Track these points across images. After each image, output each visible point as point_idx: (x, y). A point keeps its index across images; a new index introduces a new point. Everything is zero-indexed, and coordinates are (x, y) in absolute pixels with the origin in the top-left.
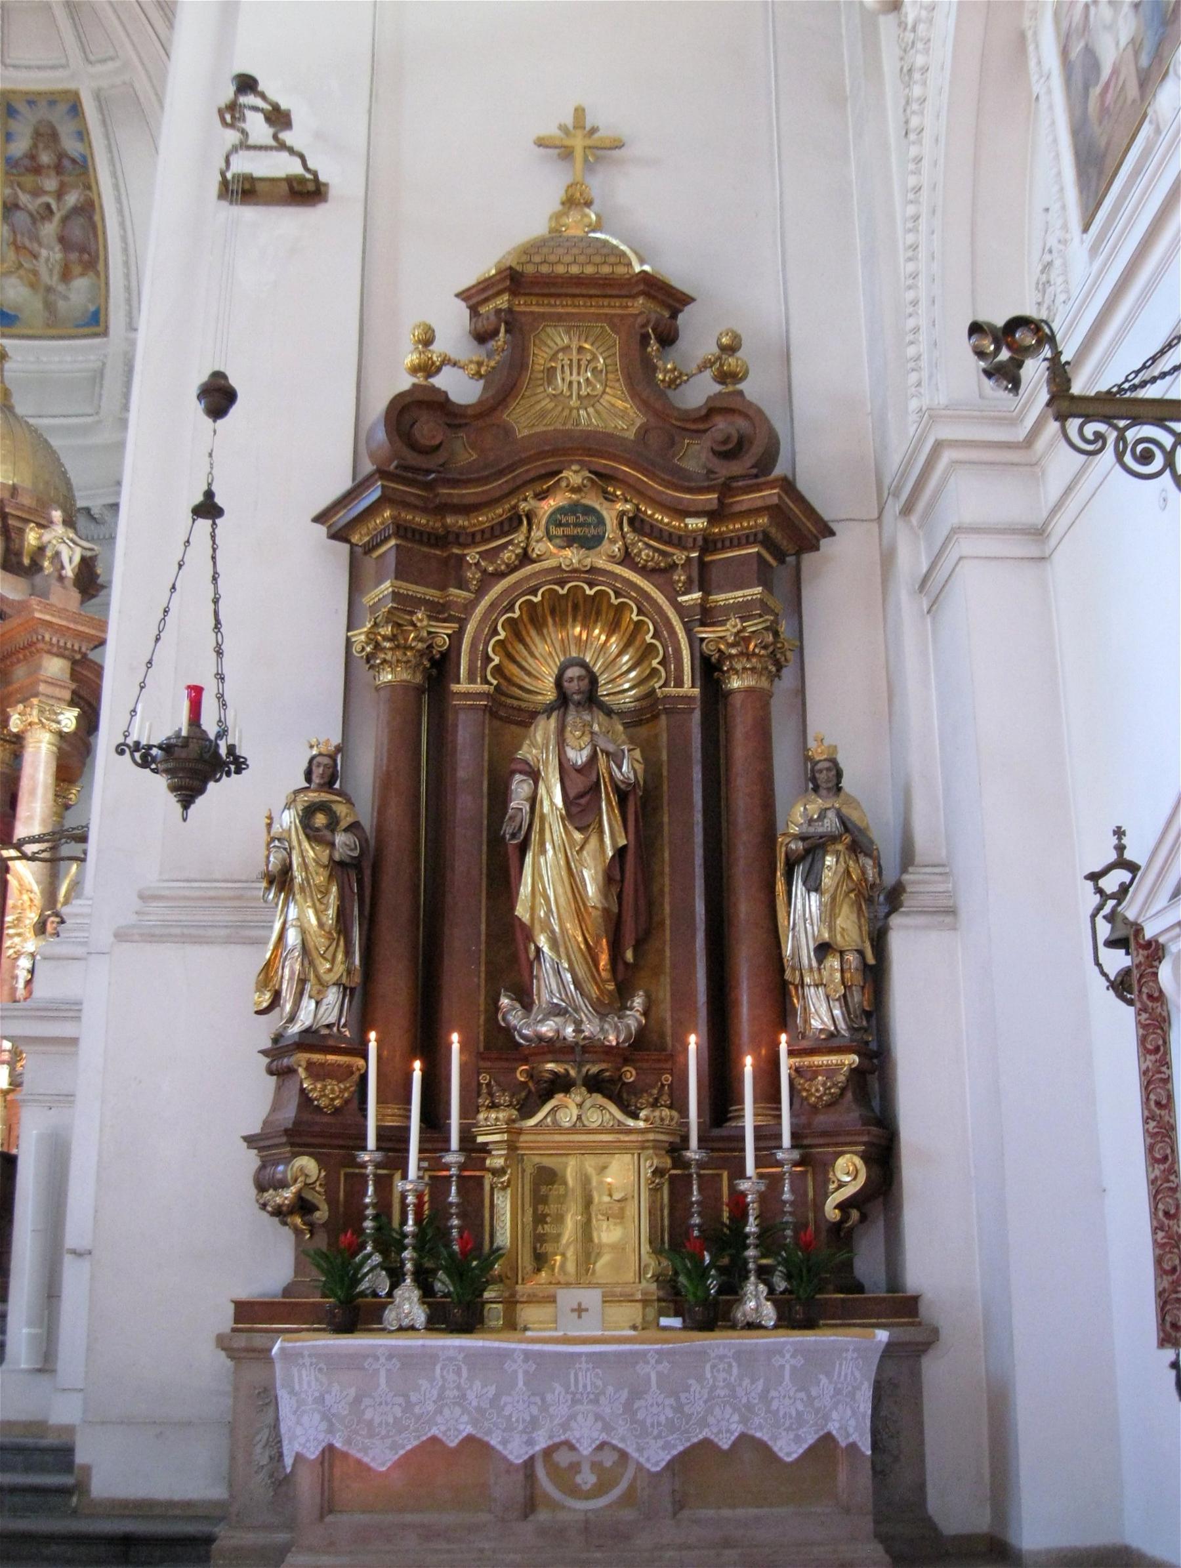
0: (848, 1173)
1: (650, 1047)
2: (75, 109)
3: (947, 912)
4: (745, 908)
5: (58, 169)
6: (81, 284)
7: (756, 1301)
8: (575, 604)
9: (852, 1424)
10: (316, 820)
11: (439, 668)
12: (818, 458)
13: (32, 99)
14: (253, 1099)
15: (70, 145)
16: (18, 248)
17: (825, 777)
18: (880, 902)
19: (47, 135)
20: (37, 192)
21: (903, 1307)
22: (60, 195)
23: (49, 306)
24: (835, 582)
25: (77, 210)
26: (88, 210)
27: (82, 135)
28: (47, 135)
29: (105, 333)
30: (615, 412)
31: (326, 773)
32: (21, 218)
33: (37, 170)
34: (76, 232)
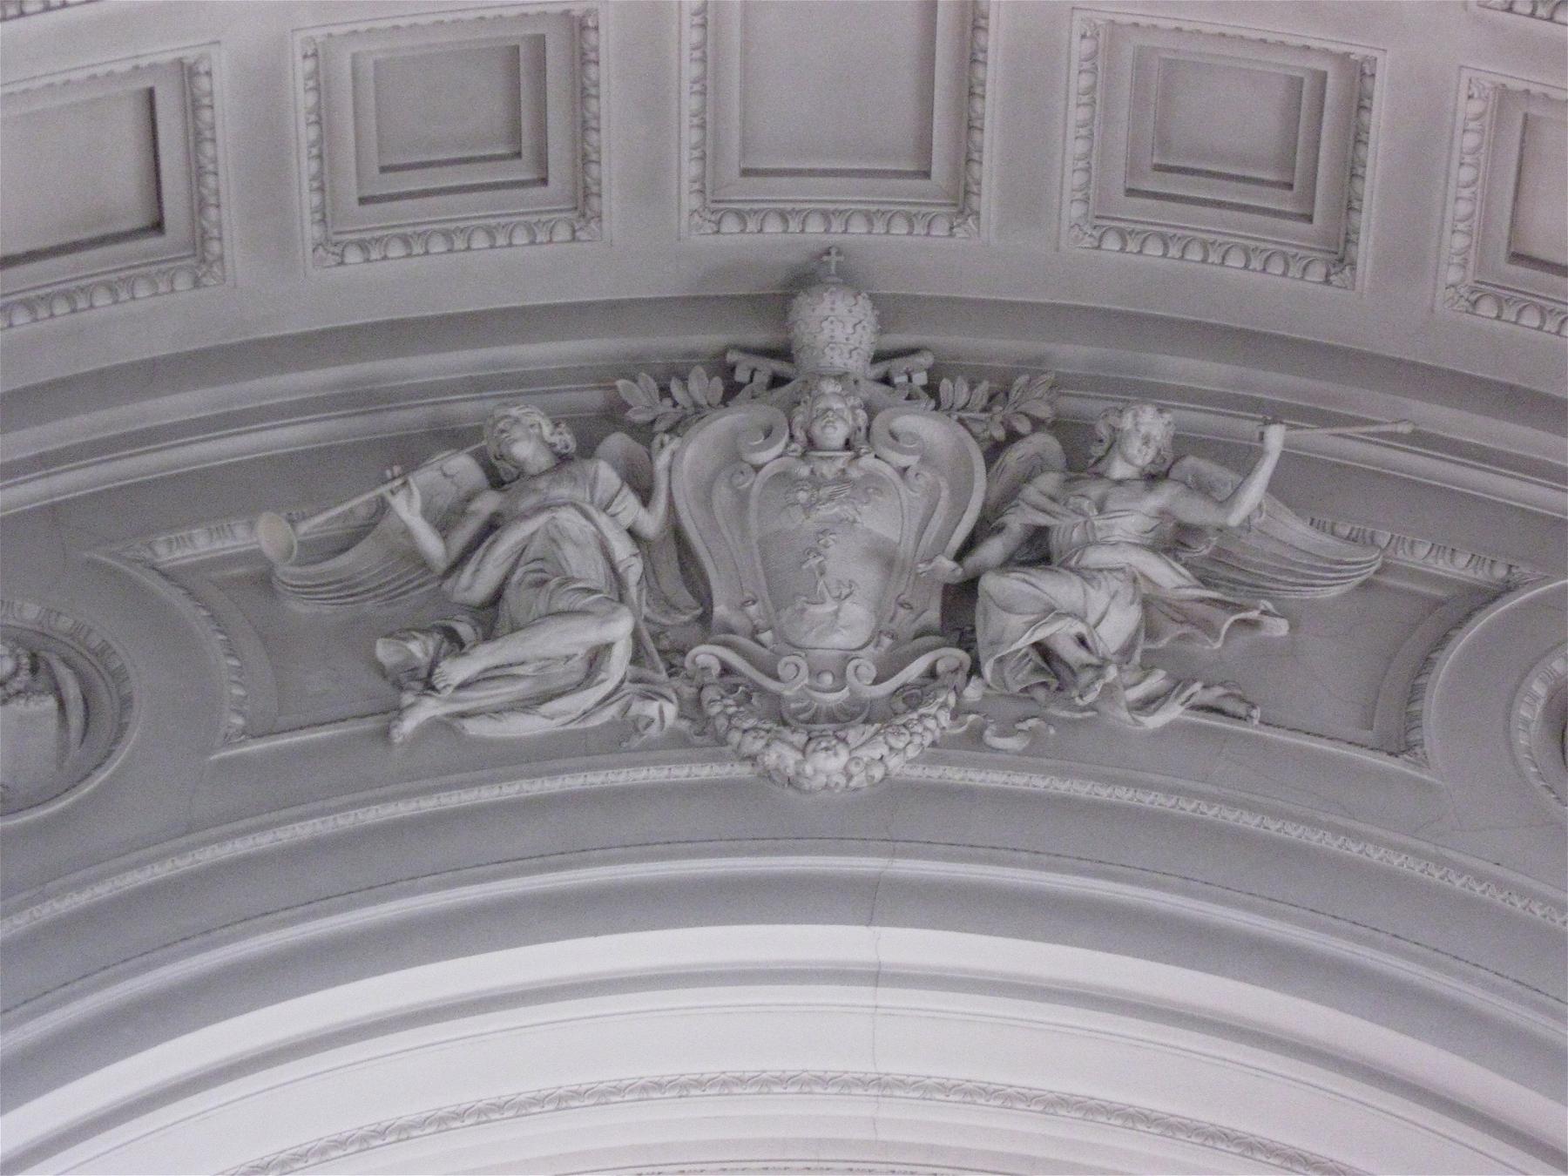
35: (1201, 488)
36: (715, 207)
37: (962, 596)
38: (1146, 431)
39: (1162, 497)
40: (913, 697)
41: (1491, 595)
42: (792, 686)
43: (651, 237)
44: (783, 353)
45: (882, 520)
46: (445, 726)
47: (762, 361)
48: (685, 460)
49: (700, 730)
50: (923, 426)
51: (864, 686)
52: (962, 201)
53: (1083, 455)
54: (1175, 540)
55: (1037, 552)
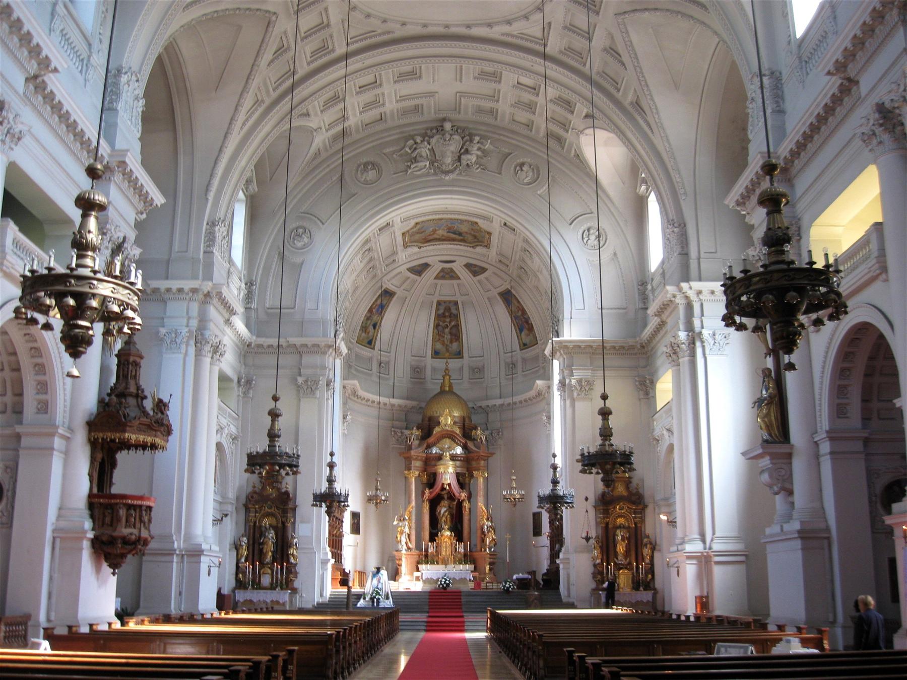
1: (630, 564)
2: (456, 303)
3: (660, 550)
4: (639, 550)
5: (450, 317)
6: (455, 345)
7: (641, 589)
8: (621, 516)
9: (650, 599)
11: (607, 524)
13: (445, 302)
14: (591, 569)
15: (454, 311)
16: (439, 335)
17: (648, 537)
18: (653, 549)
19: (448, 309)
20: (444, 322)
21: (655, 589)
22: (450, 323)
23: (447, 350)
25: (454, 326)
26: (458, 326)
27: (458, 309)
28: (448, 309)
29: (462, 357)
30: (625, 494)
31: (597, 537)
32: (440, 328)
33: (445, 317)
34: (454, 331)
35: (482, 144)
36: (435, 113)
38: (477, 139)
39: (479, 145)
40: (455, 169)
41: (510, 154)
42: (444, 168)
43: (429, 115)
44: (442, 126)
45: (452, 148)
46: (412, 173)
48: (433, 141)
49: (435, 174)
50: (457, 137)
51: (451, 168)
52: (459, 113)
53: (471, 141)
54: (479, 149)
55: (467, 152)
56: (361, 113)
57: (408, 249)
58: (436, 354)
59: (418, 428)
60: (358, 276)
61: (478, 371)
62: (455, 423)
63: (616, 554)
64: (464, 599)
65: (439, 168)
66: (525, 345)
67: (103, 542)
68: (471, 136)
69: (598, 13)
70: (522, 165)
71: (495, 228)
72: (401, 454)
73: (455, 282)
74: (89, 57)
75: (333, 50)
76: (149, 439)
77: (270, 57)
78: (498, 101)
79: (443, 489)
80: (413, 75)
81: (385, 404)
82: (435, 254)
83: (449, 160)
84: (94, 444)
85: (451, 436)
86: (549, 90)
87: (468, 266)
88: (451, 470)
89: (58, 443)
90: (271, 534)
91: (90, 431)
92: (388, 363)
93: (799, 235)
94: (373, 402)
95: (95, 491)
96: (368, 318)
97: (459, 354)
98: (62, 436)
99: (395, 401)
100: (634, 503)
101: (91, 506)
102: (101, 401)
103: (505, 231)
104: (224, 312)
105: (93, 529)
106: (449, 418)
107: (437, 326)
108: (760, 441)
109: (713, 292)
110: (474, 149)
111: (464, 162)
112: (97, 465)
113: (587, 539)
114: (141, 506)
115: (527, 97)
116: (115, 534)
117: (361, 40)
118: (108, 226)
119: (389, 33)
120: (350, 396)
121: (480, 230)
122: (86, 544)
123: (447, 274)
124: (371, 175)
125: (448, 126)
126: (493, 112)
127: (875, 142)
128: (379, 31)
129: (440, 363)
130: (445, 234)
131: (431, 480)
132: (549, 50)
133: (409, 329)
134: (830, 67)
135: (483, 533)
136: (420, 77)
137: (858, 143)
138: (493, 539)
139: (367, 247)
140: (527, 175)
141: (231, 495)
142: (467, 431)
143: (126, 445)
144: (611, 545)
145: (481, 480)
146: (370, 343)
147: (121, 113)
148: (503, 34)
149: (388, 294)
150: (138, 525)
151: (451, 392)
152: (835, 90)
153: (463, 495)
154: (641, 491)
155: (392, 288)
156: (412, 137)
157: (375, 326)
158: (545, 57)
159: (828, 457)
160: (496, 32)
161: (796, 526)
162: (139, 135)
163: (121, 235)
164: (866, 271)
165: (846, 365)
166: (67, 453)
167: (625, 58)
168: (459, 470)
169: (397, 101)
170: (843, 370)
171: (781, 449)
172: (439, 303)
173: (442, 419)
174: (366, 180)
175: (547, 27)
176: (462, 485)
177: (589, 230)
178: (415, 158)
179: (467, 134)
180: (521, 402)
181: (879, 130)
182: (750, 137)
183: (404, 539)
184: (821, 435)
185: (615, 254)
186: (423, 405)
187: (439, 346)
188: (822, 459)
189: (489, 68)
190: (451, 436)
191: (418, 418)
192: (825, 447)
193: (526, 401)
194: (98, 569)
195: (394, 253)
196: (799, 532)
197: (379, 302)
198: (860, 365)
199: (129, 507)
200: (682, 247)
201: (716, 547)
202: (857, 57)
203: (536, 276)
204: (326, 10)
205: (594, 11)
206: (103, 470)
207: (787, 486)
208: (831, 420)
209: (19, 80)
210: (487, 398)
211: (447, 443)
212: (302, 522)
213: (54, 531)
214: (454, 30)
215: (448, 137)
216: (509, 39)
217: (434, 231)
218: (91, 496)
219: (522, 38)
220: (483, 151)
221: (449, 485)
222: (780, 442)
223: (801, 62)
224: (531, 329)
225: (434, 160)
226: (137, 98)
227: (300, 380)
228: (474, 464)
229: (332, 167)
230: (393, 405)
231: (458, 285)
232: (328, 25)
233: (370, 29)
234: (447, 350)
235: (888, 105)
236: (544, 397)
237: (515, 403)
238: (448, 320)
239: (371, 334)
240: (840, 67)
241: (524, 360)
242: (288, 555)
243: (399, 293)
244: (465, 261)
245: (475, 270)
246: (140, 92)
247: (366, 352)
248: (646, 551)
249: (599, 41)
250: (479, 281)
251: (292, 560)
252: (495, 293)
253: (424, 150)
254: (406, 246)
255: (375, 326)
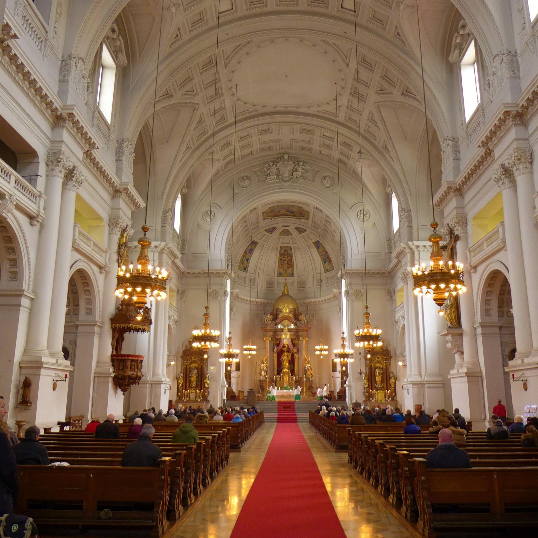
0: (394, 394)
2: (290, 248)
6: (290, 270)
10: (366, 376)
11: (371, 366)
12: (392, 354)
13: (284, 247)
14: (363, 390)
15: (289, 252)
17: (393, 373)
18: (396, 379)
19: (286, 251)
22: (287, 258)
23: (286, 273)
24: (392, 360)
26: (291, 260)
27: (291, 251)
28: (286, 251)
29: (294, 276)
31: (366, 373)
34: (289, 262)
36: (279, 149)
37: (292, 173)
38: (301, 163)
42: (284, 179)
47: (282, 158)
49: (280, 182)
50: (290, 162)
51: (288, 179)
52: (292, 149)
53: (298, 164)
54: (303, 169)
55: (296, 170)
56: (241, 151)
57: (266, 220)
58: (280, 275)
59: (271, 314)
60: (239, 235)
61: (302, 284)
62: (290, 311)
63: (376, 383)
64: (296, 406)
65: (281, 179)
66: (327, 270)
67: (118, 378)
68: (298, 162)
69: (365, 102)
70: (325, 177)
71: (311, 210)
72: (261, 328)
73: (290, 237)
74: (109, 136)
75: (227, 120)
76: (142, 327)
77: (195, 125)
78: (312, 144)
79: (284, 347)
80: (268, 131)
81: (253, 302)
82: (279, 223)
83: (286, 175)
84: (114, 329)
85: (288, 318)
86: (339, 139)
87: (297, 228)
88: (288, 337)
89: (96, 329)
90: (195, 372)
91: (112, 323)
92: (255, 279)
93: (466, 223)
94: (247, 300)
95: (115, 353)
96: (244, 256)
97: (292, 275)
98: (99, 326)
99: (259, 300)
100: (385, 355)
101: (113, 360)
102: (118, 308)
103: (316, 211)
104: (172, 257)
105: (114, 372)
106: (286, 310)
107: (281, 259)
108: (447, 327)
109: (425, 246)
110: (300, 169)
111: (295, 176)
112: (115, 340)
113: (361, 373)
114: (138, 360)
115: (327, 142)
116: (125, 374)
117: (242, 115)
118: (120, 220)
119: (256, 111)
120: (235, 298)
121: (304, 210)
122: (110, 380)
123: (286, 233)
124: (246, 183)
125: (286, 157)
126: (310, 150)
127: (501, 183)
128: (251, 110)
129: (282, 280)
130: (285, 212)
131: (277, 342)
132: (339, 119)
133: (265, 261)
134: (480, 143)
135: (305, 370)
136: (272, 132)
137: (492, 182)
138: (311, 374)
139: (244, 220)
140: (327, 183)
141: (174, 351)
142: (296, 316)
143: (130, 329)
144: (373, 377)
145: (304, 342)
146: (245, 269)
147: (124, 162)
148: (315, 111)
149: (254, 243)
150: (136, 370)
151: (288, 295)
152: (483, 153)
153: (295, 350)
154: (388, 348)
155: (257, 240)
156: (267, 163)
157: (247, 260)
158: (337, 122)
159: (481, 335)
160: (311, 111)
161: (465, 370)
162: (132, 172)
163: (125, 224)
164: (497, 245)
165: (489, 289)
166: (100, 335)
167: (380, 124)
168: (293, 337)
169: (260, 144)
170: (488, 292)
171: (457, 331)
172: (281, 248)
173: (284, 310)
174: (243, 185)
175: (338, 108)
176: (294, 345)
177: (360, 211)
178: (269, 174)
179: (296, 161)
180: (325, 300)
181: (503, 177)
182: (443, 170)
183: (263, 373)
184: (477, 325)
185: (374, 224)
186: (273, 302)
187: (281, 270)
188: (478, 336)
189: (307, 127)
190: (288, 318)
191: (270, 309)
192: (479, 331)
193: (327, 299)
194: (116, 393)
195: (258, 222)
196: (466, 373)
197: (249, 248)
198: (497, 289)
199: (132, 361)
200: (409, 223)
201: (426, 379)
202: (493, 139)
203: (333, 235)
204: (224, 101)
205: (363, 101)
206: (118, 342)
207: (460, 350)
208: (482, 318)
209: (80, 154)
210: (307, 298)
211: (286, 322)
212: (212, 365)
213: (95, 373)
214: (290, 109)
215: (286, 162)
216: (319, 114)
217: (279, 211)
218: (112, 355)
219: (325, 113)
220: (305, 170)
221: (287, 345)
222: (457, 328)
223: (467, 135)
224: (330, 261)
225: (279, 175)
226: (131, 154)
227: (210, 291)
228: (300, 333)
229: (225, 179)
230: (257, 302)
231: (292, 238)
232: (225, 108)
233: (246, 109)
234: (286, 273)
235: (506, 165)
236: (337, 298)
237: (322, 301)
238: (286, 256)
239: (245, 264)
240: (484, 144)
241: (327, 278)
242: (204, 383)
243: (260, 242)
244: (295, 226)
245: (300, 230)
246: (132, 150)
247: (243, 274)
248: (392, 380)
249: (365, 115)
250: (302, 236)
251: (206, 386)
252: (311, 242)
253: (274, 170)
254: (264, 219)
255: (247, 260)
